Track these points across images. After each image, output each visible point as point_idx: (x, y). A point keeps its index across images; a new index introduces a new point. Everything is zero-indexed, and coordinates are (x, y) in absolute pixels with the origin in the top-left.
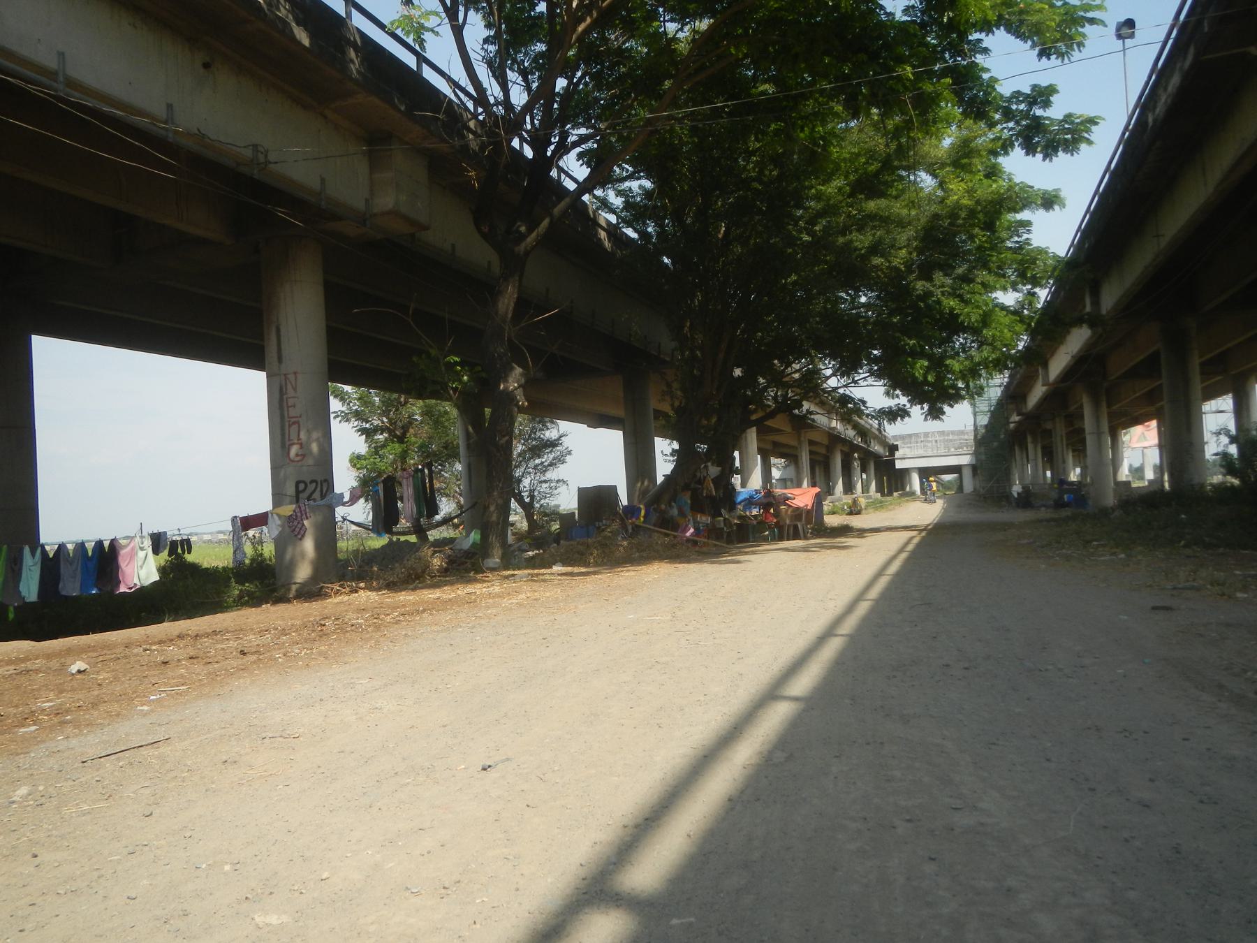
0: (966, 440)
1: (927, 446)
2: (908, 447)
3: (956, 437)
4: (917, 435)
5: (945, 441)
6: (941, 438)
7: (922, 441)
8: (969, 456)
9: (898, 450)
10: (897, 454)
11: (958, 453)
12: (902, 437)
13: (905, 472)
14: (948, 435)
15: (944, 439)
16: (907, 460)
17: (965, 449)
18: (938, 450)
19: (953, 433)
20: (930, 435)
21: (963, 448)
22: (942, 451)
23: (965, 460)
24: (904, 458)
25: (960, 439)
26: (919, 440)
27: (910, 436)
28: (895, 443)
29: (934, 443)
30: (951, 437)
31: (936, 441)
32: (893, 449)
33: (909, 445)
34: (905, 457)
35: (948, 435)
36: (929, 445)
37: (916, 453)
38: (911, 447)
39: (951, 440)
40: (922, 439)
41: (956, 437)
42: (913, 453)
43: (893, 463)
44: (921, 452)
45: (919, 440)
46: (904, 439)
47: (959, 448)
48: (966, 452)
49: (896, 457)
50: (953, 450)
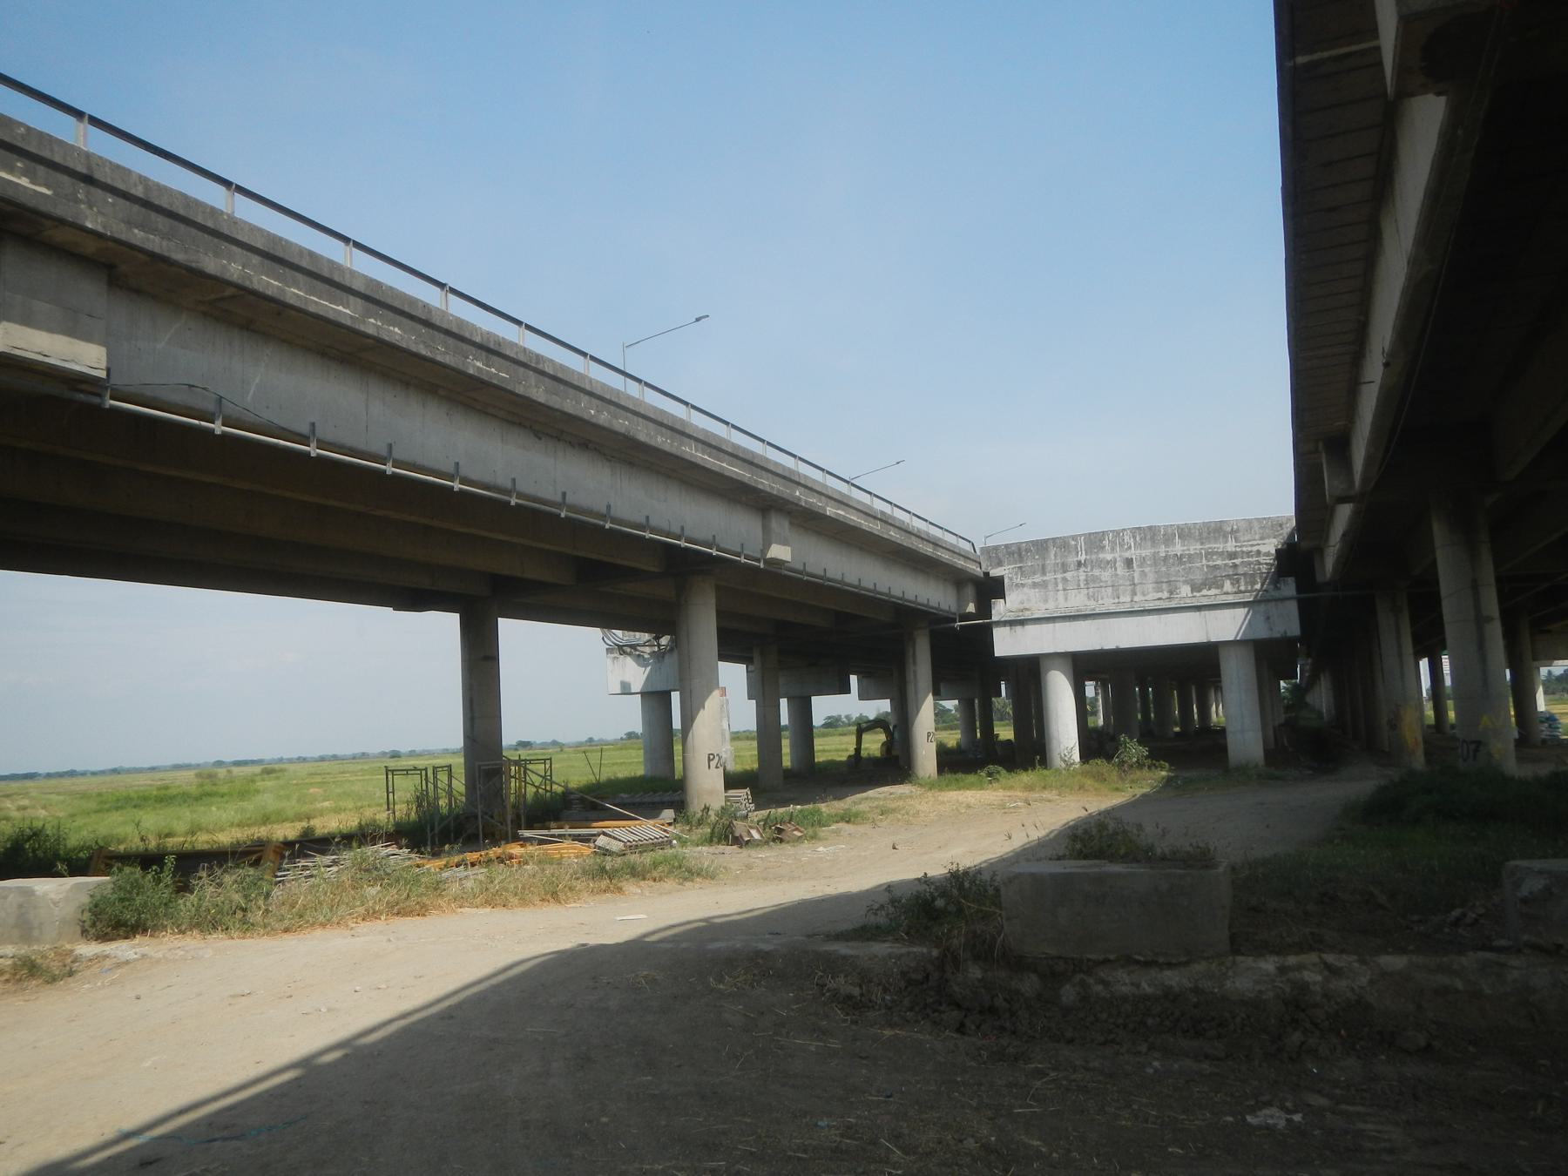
0: (1233, 555)
1: (1096, 579)
2: (1035, 585)
3: (1194, 547)
4: (1063, 544)
5: (1155, 559)
6: (1145, 553)
7: (1079, 564)
8: (1242, 611)
9: (1003, 596)
10: (999, 609)
11: (1205, 602)
12: (1016, 553)
13: (1028, 672)
14: (1168, 540)
15: (1155, 556)
16: (1030, 628)
17: (1228, 586)
18: (1134, 593)
19: (1185, 533)
20: (1106, 542)
21: (1223, 586)
22: (1150, 596)
23: (1226, 626)
24: (1022, 622)
25: (1210, 554)
26: (1072, 559)
27: (1041, 546)
28: (995, 572)
29: (1120, 571)
30: (1178, 548)
31: (1129, 563)
32: (991, 589)
33: (1038, 578)
34: (1027, 615)
35: (1168, 540)
36: (1106, 575)
37: (1062, 603)
38: (1044, 585)
39: (1179, 558)
40: (1082, 558)
41: (1194, 547)
42: (1051, 605)
43: (983, 636)
44: (1077, 601)
45: (1072, 559)
46: (1021, 559)
47: (1215, 583)
48: (1231, 599)
49: (994, 618)
50: (1185, 590)
